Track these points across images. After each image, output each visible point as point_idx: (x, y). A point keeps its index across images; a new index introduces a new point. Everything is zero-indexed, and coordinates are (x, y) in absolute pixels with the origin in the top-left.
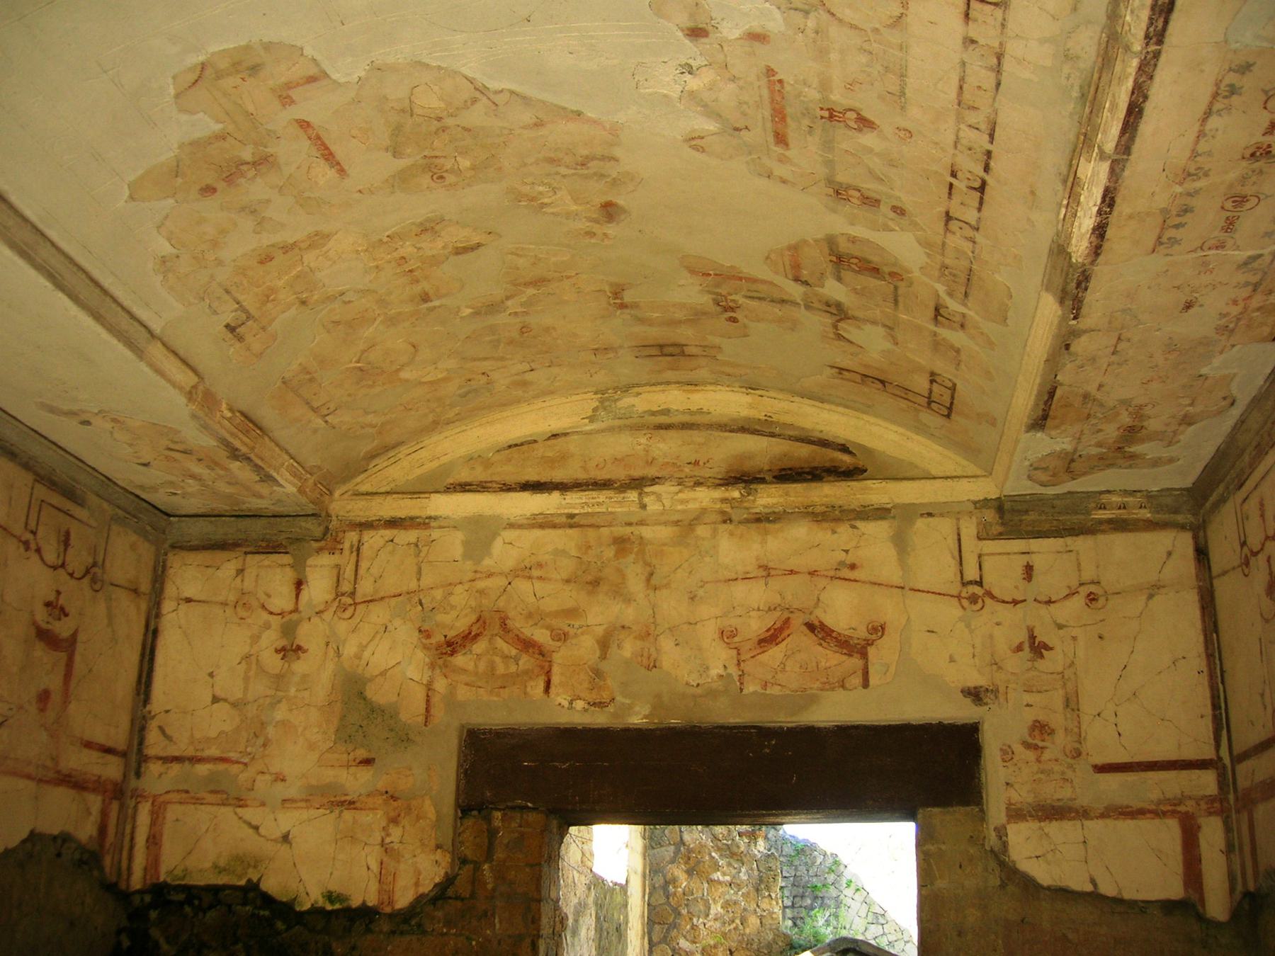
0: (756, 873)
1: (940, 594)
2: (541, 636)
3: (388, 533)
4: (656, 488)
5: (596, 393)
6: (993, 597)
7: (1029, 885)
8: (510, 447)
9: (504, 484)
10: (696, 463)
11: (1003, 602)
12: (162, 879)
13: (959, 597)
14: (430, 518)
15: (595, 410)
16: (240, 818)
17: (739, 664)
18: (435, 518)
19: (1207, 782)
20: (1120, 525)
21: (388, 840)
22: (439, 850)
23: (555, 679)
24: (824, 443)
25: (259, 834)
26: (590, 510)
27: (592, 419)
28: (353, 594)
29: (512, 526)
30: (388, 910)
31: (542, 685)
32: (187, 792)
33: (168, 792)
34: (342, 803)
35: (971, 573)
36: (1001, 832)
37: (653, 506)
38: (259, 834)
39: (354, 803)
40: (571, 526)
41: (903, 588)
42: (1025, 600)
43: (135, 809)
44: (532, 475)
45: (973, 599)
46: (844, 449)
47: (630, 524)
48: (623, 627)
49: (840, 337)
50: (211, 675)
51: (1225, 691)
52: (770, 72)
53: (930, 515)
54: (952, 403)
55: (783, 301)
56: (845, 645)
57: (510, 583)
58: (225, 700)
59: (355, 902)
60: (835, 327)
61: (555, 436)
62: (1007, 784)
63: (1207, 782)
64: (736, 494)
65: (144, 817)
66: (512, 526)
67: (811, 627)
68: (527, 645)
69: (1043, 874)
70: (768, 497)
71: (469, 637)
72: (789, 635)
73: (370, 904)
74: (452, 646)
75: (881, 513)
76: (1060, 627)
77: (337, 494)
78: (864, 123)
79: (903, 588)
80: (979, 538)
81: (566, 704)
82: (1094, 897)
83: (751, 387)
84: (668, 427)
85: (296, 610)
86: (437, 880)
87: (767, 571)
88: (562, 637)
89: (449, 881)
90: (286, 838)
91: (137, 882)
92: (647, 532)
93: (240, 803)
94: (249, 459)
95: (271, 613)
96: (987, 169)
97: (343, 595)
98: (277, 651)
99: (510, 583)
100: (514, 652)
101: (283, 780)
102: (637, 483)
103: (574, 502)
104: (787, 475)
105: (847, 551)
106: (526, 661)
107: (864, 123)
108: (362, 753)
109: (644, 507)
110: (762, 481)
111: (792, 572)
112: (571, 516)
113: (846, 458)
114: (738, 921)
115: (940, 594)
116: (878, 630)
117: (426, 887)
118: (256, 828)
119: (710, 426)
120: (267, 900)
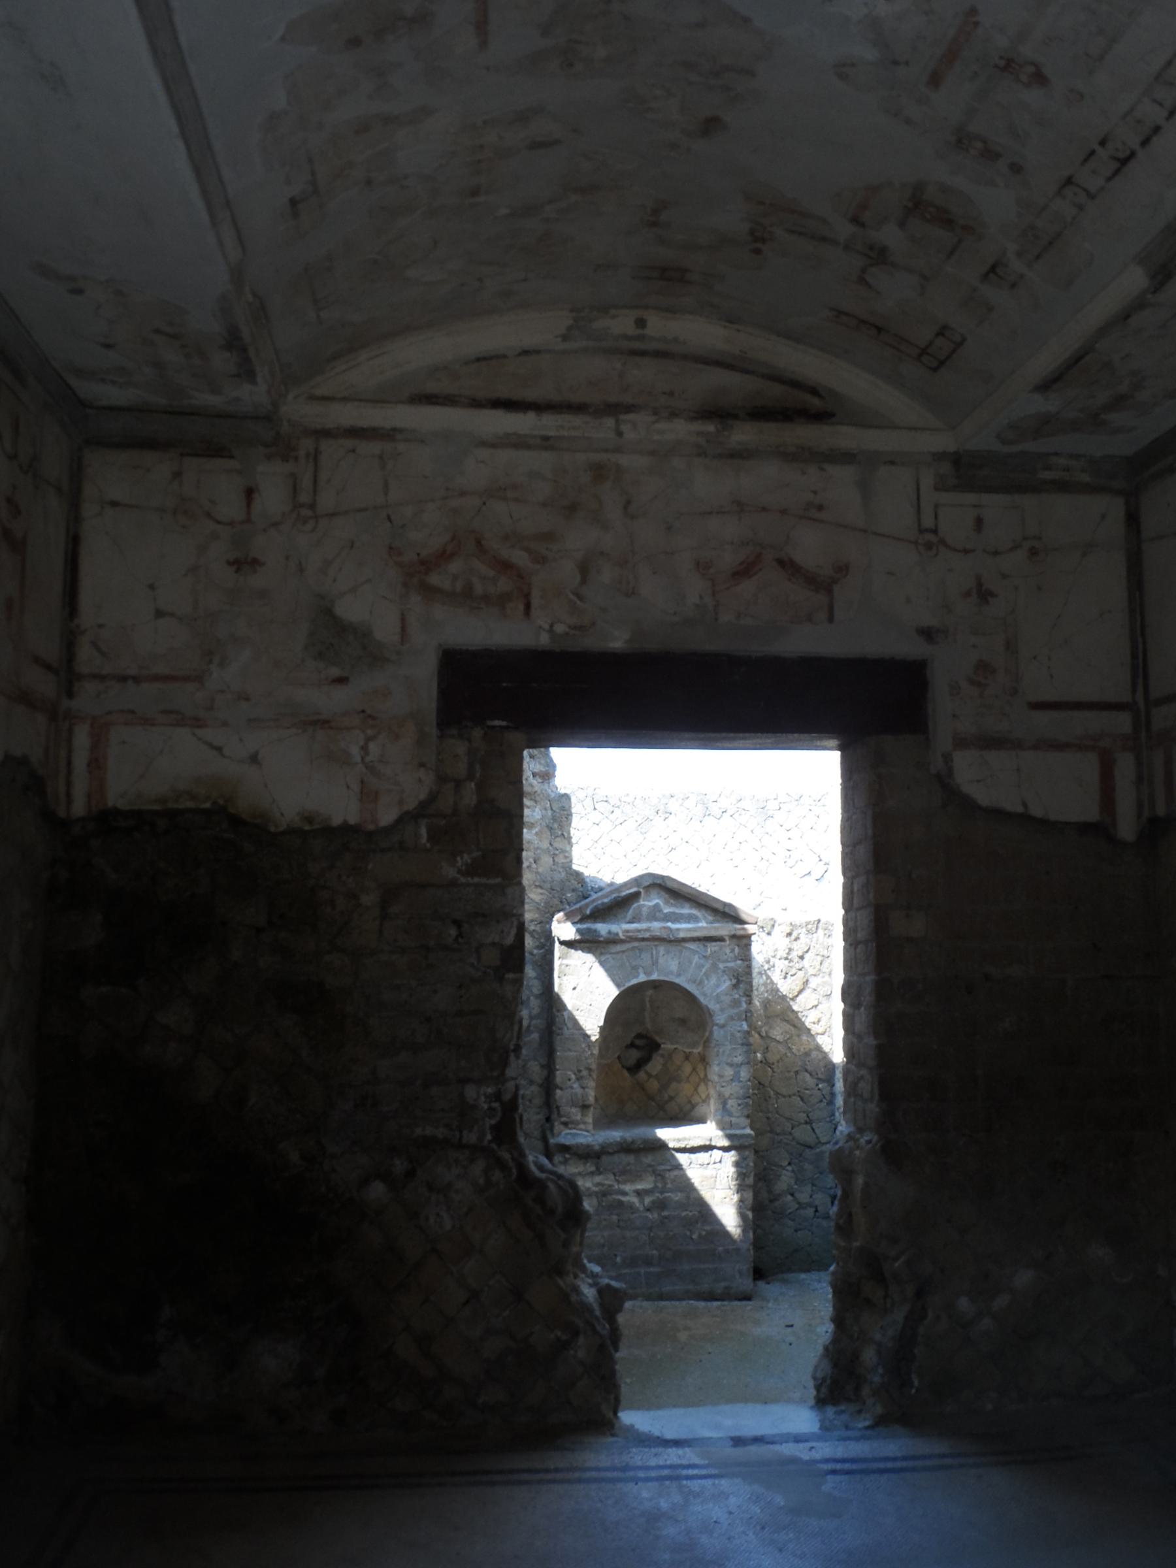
0: (550, 813)
1: (899, 539)
2: (519, 557)
3: (349, 443)
4: (631, 416)
5: (572, 311)
6: (947, 546)
7: (968, 806)
8: (478, 360)
9: (474, 400)
10: (671, 394)
11: (955, 550)
12: (110, 804)
13: (916, 543)
14: (394, 430)
15: (569, 328)
16: (200, 739)
17: (714, 594)
18: (401, 431)
19: (1123, 722)
20: (1062, 486)
21: (368, 759)
22: (422, 769)
23: (536, 602)
24: (795, 384)
25: (223, 756)
26: (566, 434)
27: (565, 338)
28: (312, 506)
29: (483, 444)
30: (371, 827)
31: (521, 607)
32: (133, 712)
33: (110, 713)
34: (314, 723)
35: (928, 522)
36: (947, 758)
37: (629, 434)
38: (223, 756)
39: (327, 722)
40: (546, 448)
41: (865, 531)
42: (973, 551)
43: (70, 731)
44: (504, 392)
45: (929, 546)
46: (814, 391)
47: (606, 451)
48: (602, 553)
49: (862, 280)
50: (152, 587)
51: (1144, 643)
52: (973, 11)
53: (892, 463)
54: (948, 357)
55: (824, 239)
56: (813, 581)
57: (484, 504)
58: (172, 615)
59: (337, 821)
60: (864, 270)
61: (525, 352)
62: (954, 716)
63: (1123, 722)
64: (711, 428)
65: (82, 738)
66: (483, 444)
67: (781, 563)
68: (505, 566)
69: (983, 796)
70: (743, 434)
71: (444, 556)
72: (760, 570)
73: (352, 822)
74: (427, 565)
75: (846, 457)
76: (1005, 576)
77: (290, 397)
78: (1039, 78)
79: (865, 531)
80: (937, 489)
81: (547, 627)
82: (1025, 818)
83: (731, 319)
84: (643, 353)
85: (248, 520)
86: (422, 797)
87: (740, 507)
88: (541, 560)
89: (432, 798)
90: (254, 759)
91: (79, 808)
92: (624, 460)
93: (198, 723)
94: (244, 350)
95: (219, 522)
96: (1145, 142)
97: (302, 506)
98: (229, 563)
99: (484, 504)
100: (492, 573)
101: (247, 699)
102: (613, 409)
103: (549, 424)
104: (762, 413)
105: (815, 493)
106: (504, 584)
107: (1039, 78)
108: (335, 672)
109: (620, 434)
110: (736, 417)
111: (764, 509)
112: (546, 438)
113: (816, 401)
114: (531, 860)
115: (899, 539)
116: (843, 569)
117: (411, 805)
118: (219, 749)
119: (685, 357)
120: (236, 821)
